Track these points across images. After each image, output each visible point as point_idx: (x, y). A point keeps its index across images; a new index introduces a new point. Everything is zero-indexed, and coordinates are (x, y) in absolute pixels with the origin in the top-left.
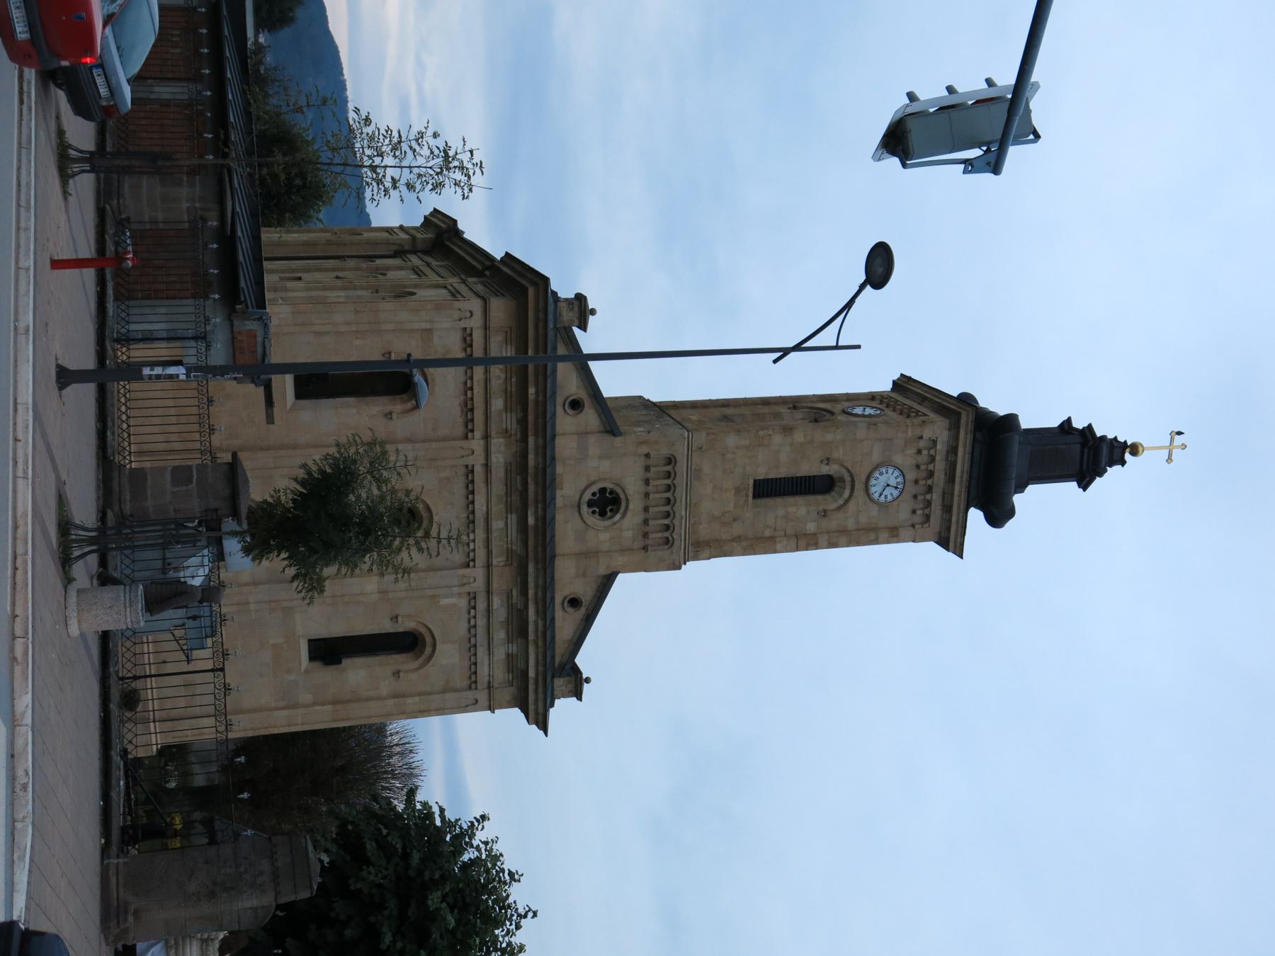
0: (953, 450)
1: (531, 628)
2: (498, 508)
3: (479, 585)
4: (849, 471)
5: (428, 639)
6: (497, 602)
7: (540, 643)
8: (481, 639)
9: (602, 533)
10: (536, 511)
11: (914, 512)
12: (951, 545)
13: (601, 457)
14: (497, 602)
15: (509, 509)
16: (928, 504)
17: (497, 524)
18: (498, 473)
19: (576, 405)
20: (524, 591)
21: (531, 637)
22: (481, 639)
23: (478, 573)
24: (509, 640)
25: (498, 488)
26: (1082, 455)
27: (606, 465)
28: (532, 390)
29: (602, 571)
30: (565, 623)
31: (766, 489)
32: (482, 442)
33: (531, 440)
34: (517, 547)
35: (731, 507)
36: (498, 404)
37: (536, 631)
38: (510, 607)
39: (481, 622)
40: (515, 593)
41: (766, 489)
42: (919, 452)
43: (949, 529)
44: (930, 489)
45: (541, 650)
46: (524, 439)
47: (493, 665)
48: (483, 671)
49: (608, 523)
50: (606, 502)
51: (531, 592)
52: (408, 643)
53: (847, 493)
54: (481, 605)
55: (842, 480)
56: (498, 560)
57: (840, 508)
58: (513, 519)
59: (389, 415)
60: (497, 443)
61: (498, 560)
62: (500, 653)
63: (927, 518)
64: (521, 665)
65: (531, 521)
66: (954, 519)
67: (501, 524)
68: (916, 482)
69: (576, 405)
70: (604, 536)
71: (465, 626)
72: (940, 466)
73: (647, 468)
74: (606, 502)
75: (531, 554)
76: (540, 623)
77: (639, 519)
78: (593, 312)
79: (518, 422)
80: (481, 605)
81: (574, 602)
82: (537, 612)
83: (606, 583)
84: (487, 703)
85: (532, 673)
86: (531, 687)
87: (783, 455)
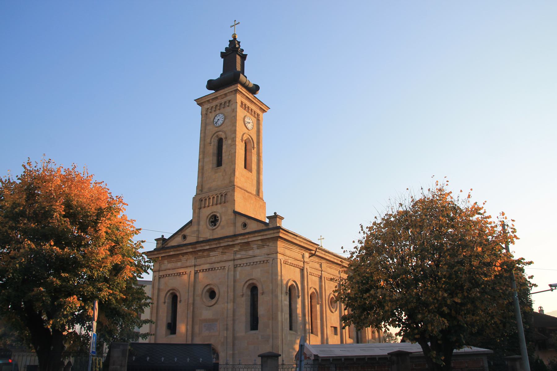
0: (208, 101)
1: (243, 241)
2: (209, 260)
3: (231, 264)
4: (214, 135)
5: (251, 282)
6: (238, 256)
7: (247, 237)
8: (251, 260)
9: (223, 220)
10: (204, 246)
11: (228, 106)
12: (235, 89)
13: (199, 224)
14: (238, 256)
15: (209, 256)
16: (225, 102)
17: (214, 259)
18: (199, 261)
19: (185, 237)
20: (233, 246)
21: (246, 241)
22: (251, 260)
23: (227, 264)
24: (252, 249)
25: (202, 260)
26: (233, 54)
27: (202, 223)
28: (171, 253)
29: (232, 216)
30: (253, 227)
31: (219, 163)
32: (188, 268)
33: (184, 251)
34: (220, 250)
35: (221, 173)
36: (179, 264)
37: (243, 239)
38: (240, 250)
39: (245, 261)
40: (235, 250)
41: (219, 163)
42: (211, 112)
43: (231, 92)
44: (221, 104)
45: (249, 236)
46: (186, 253)
47: (259, 253)
48: (262, 258)
49: (219, 218)
50: (214, 220)
51: (231, 243)
52: (254, 289)
53: (220, 133)
54: (239, 262)
55: (217, 136)
56: (225, 257)
57: (225, 132)
58: (212, 254)
59: (180, 301)
60: (188, 264)
61: (225, 257)
62: (257, 252)
63: (229, 101)
64: (260, 243)
65: (208, 247)
66: (227, 92)
67: (214, 258)
68: (219, 109)
69: (185, 237)
70: (223, 219)
71: (247, 267)
72: (214, 103)
73: (204, 207)
74: (214, 220)
75: (218, 246)
76: (240, 238)
77: (219, 206)
78: (163, 236)
79: (183, 256)
80: (239, 262)
81: (245, 225)
82: (237, 240)
83: (236, 213)
84: (275, 255)
85: (260, 238)
86: (265, 237)
87: (211, 159)
